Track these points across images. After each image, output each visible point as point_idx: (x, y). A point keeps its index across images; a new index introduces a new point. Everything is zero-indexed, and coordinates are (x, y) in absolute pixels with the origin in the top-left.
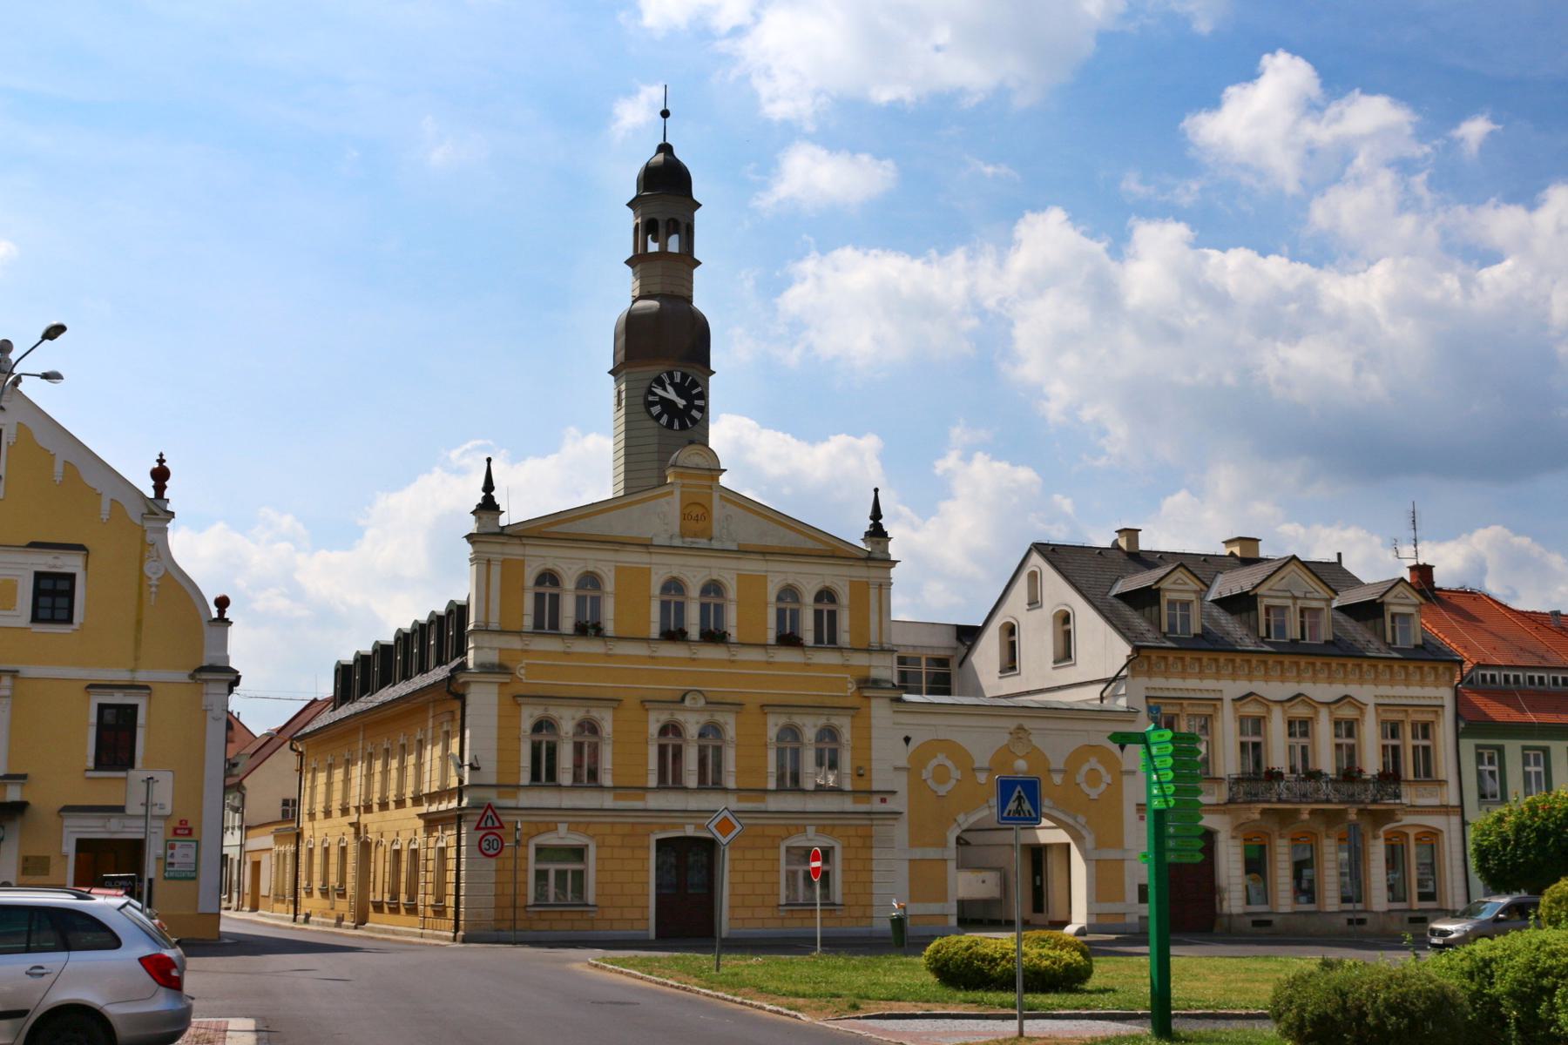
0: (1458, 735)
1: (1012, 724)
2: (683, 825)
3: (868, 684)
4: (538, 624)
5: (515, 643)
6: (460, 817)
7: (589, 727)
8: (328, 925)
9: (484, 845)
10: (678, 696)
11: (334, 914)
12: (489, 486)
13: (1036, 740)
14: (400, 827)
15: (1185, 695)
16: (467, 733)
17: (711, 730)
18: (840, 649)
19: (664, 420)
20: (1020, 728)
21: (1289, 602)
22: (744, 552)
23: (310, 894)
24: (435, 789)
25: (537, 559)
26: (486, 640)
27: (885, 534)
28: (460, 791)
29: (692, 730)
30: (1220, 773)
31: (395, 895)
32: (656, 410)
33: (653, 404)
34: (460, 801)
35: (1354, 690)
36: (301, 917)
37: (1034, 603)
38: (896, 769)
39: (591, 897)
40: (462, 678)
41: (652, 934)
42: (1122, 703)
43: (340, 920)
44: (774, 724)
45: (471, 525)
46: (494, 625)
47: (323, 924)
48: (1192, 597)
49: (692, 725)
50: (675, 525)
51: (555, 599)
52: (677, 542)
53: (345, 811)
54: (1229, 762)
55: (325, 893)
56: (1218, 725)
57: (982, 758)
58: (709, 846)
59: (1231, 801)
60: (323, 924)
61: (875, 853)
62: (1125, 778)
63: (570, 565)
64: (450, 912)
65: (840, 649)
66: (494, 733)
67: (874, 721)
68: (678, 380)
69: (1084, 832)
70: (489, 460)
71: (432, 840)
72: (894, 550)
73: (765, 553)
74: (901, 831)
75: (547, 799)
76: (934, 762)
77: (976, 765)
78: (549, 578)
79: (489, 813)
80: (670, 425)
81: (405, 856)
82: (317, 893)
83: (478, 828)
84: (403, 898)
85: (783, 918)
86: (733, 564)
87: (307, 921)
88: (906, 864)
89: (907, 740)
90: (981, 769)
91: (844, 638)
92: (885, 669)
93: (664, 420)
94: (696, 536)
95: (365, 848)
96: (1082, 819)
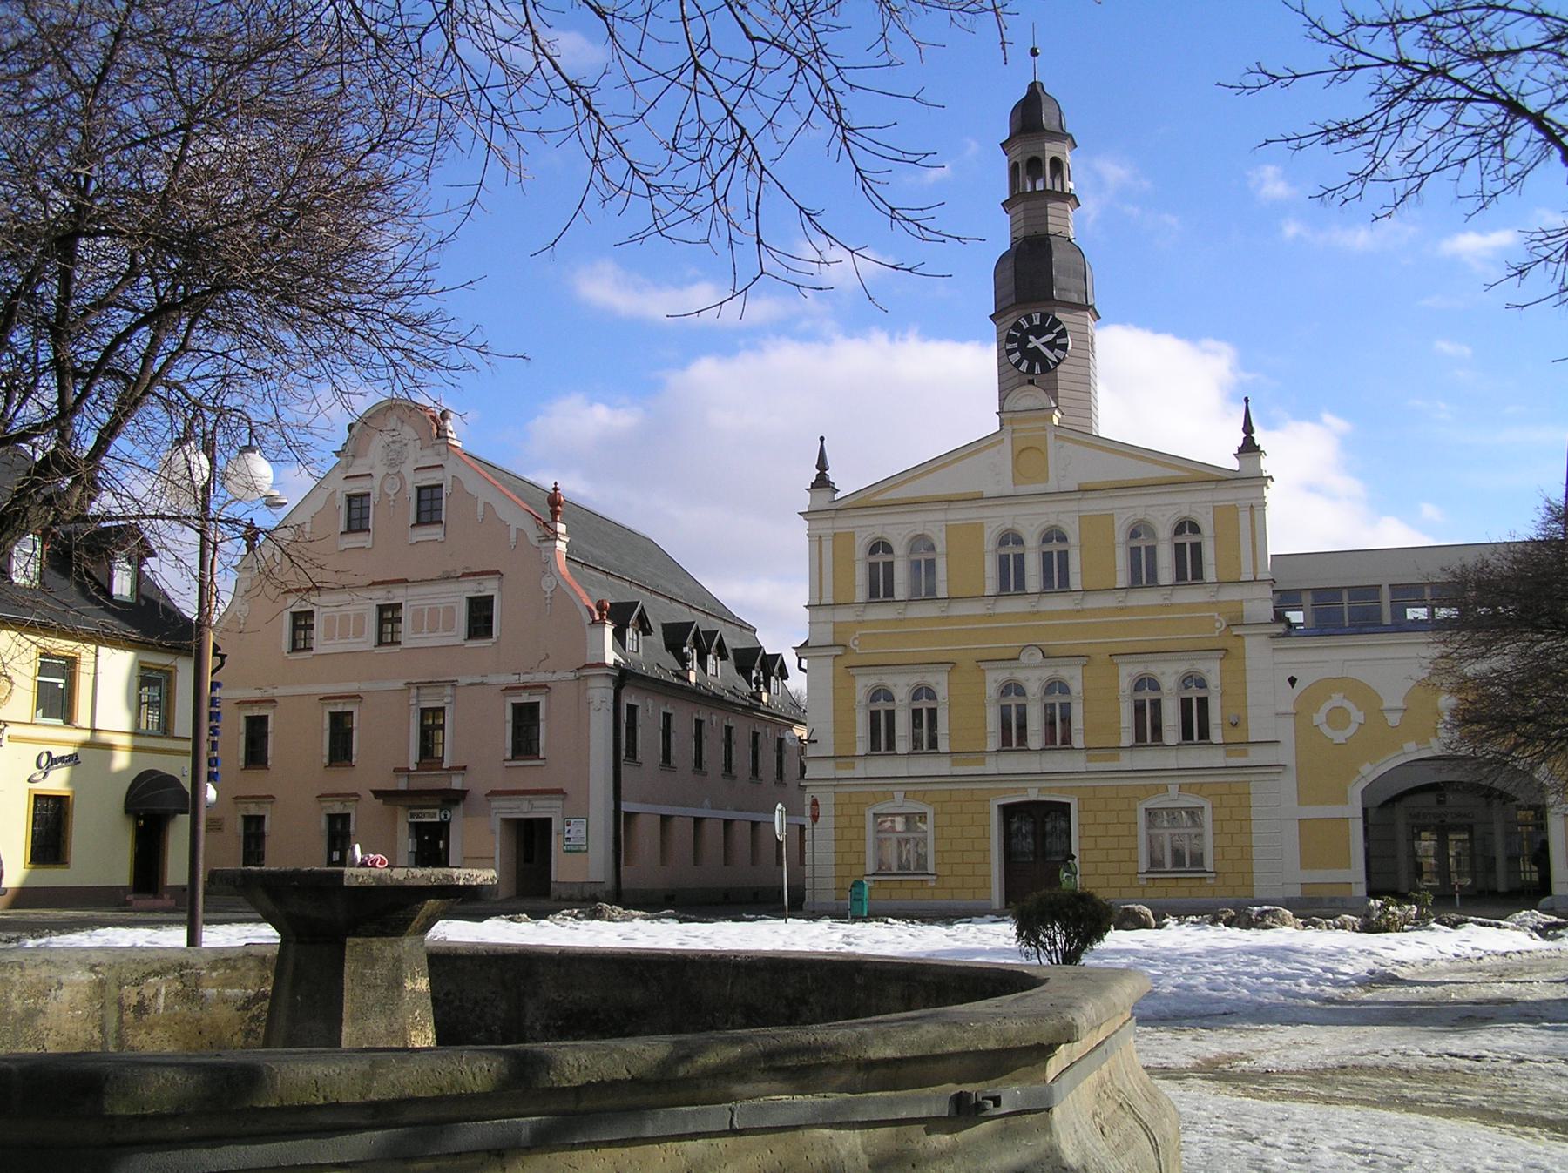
4: (873, 592)
12: (822, 465)
19: (1024, 366)
25: (866, 529)
29: (1034, 688)
44: (1127, 674)
45: (805, 501)
46: (828, 600)
58: (1064, 809)
70: (822, 439)
72: (1267, 465)
76: (1326, 706)
77: (1386, 705)
80: (1031, 369)
85: (1143, 887)
86: (1073, 506)
89: (1292, 681)
92: (1260, 605)
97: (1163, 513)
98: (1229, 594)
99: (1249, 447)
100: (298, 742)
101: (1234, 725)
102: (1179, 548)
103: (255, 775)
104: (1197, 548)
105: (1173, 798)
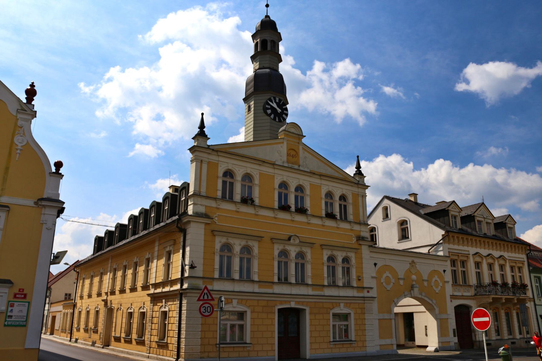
0: (530, 272)
1: (410, 260)
2: (290, 302)
3: (360, 238)
4: (224, 197)
5: (213, 204)
6: (181, 295)
7: (247, 249)
8: (87, 345)
9: (203, 310)
10: (287, 238)
11: (91, 340)
14: (139, 300)
15: (460, 252)
16: (188, 249)
17: (301, 255)
18: (350, 222)
19: (272, 116)
20: (413, 262)
21: (483, 219)
22: (312, 173)
23: (78, 330)
24: (159, 280)
25: (225, 164)
26: (200, 201)
27: (363, 175)
28: (182, 280)
29: (293, 255)
30: (471, 284)
31: (129, 332)
33: (268, 109)
34: (182, 285)
36: (73, 340)
37: (386, 216)
38: (373, 277)
40: (185, 220)
41: (277, 359)
42: (441, 253)
43: (94, 344)
44: (326, 254)
45: (193, 143)
46: (203, 194)
47: (85, 344)
48: (457, 214)
49: (293, 251)
50: (285, 159)
51: (232, 184)
52: (286, 165)
53: (99, 295)
54: (473, 280)
55: (86, 330)
56: (469, 264)
57: (401, 275)
59: (475, 295)
60: (85, 344)
61: (367, 316)
62: (446, 284)
63: (240, 170)
64: (173, 347)
65: (350, 222)
66: (202, 249)
67: (363, 255)
68: (277, 101)
69: (435, 307)
71: (156, 308)
72: (367, 181)
73: (321, 176)
74: (375, 305)
75: (227, 286)
78: (229, 174)
79: (206, 291)
80: (274, 119)
81: (136, 316)
82: (82, 330)
83: (199, 300)
84: (134, 336)
87: (76, 341)
88: (377, 321)
89: (375, 264)
90: (401, 279)
91: (351, 217)
93: (272, 116)
94: (293, 163)
95: (110, 311)
96: (434, 302)
101: (359, 280)
105: (342, 309)
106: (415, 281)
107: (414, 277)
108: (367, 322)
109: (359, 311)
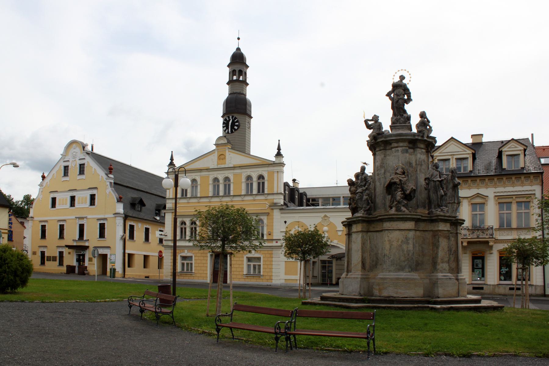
3: (274, 205)
12: (172, 159)
13: (331, 220)
20: (326, 216)
32: (236, 127)
35: (483, 191)
39: (193, 271)
86: (232, 171)
89: (285, 222)
97: (255, 174)
98: (270, 197)
99: (279, 154)
100: (53, 232)
102: (259, 184)
103: (43, 241)
104: (263, 183)
106: (327, 232)
107: (326, 228)
108: (273, 263)
109: (269, 256)
